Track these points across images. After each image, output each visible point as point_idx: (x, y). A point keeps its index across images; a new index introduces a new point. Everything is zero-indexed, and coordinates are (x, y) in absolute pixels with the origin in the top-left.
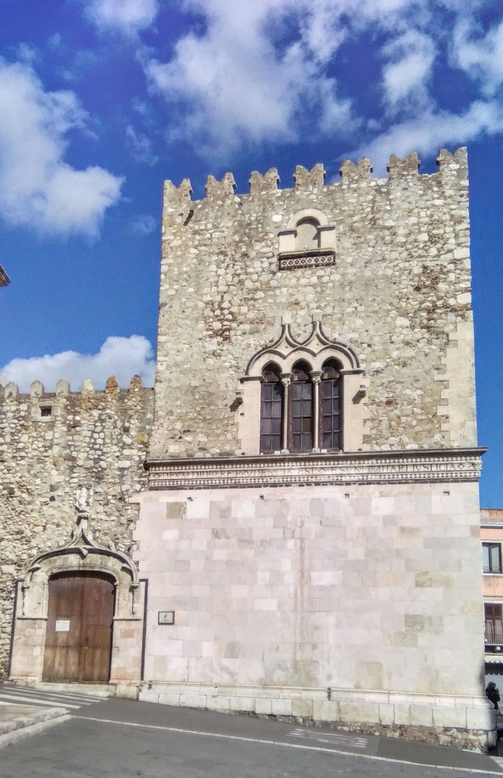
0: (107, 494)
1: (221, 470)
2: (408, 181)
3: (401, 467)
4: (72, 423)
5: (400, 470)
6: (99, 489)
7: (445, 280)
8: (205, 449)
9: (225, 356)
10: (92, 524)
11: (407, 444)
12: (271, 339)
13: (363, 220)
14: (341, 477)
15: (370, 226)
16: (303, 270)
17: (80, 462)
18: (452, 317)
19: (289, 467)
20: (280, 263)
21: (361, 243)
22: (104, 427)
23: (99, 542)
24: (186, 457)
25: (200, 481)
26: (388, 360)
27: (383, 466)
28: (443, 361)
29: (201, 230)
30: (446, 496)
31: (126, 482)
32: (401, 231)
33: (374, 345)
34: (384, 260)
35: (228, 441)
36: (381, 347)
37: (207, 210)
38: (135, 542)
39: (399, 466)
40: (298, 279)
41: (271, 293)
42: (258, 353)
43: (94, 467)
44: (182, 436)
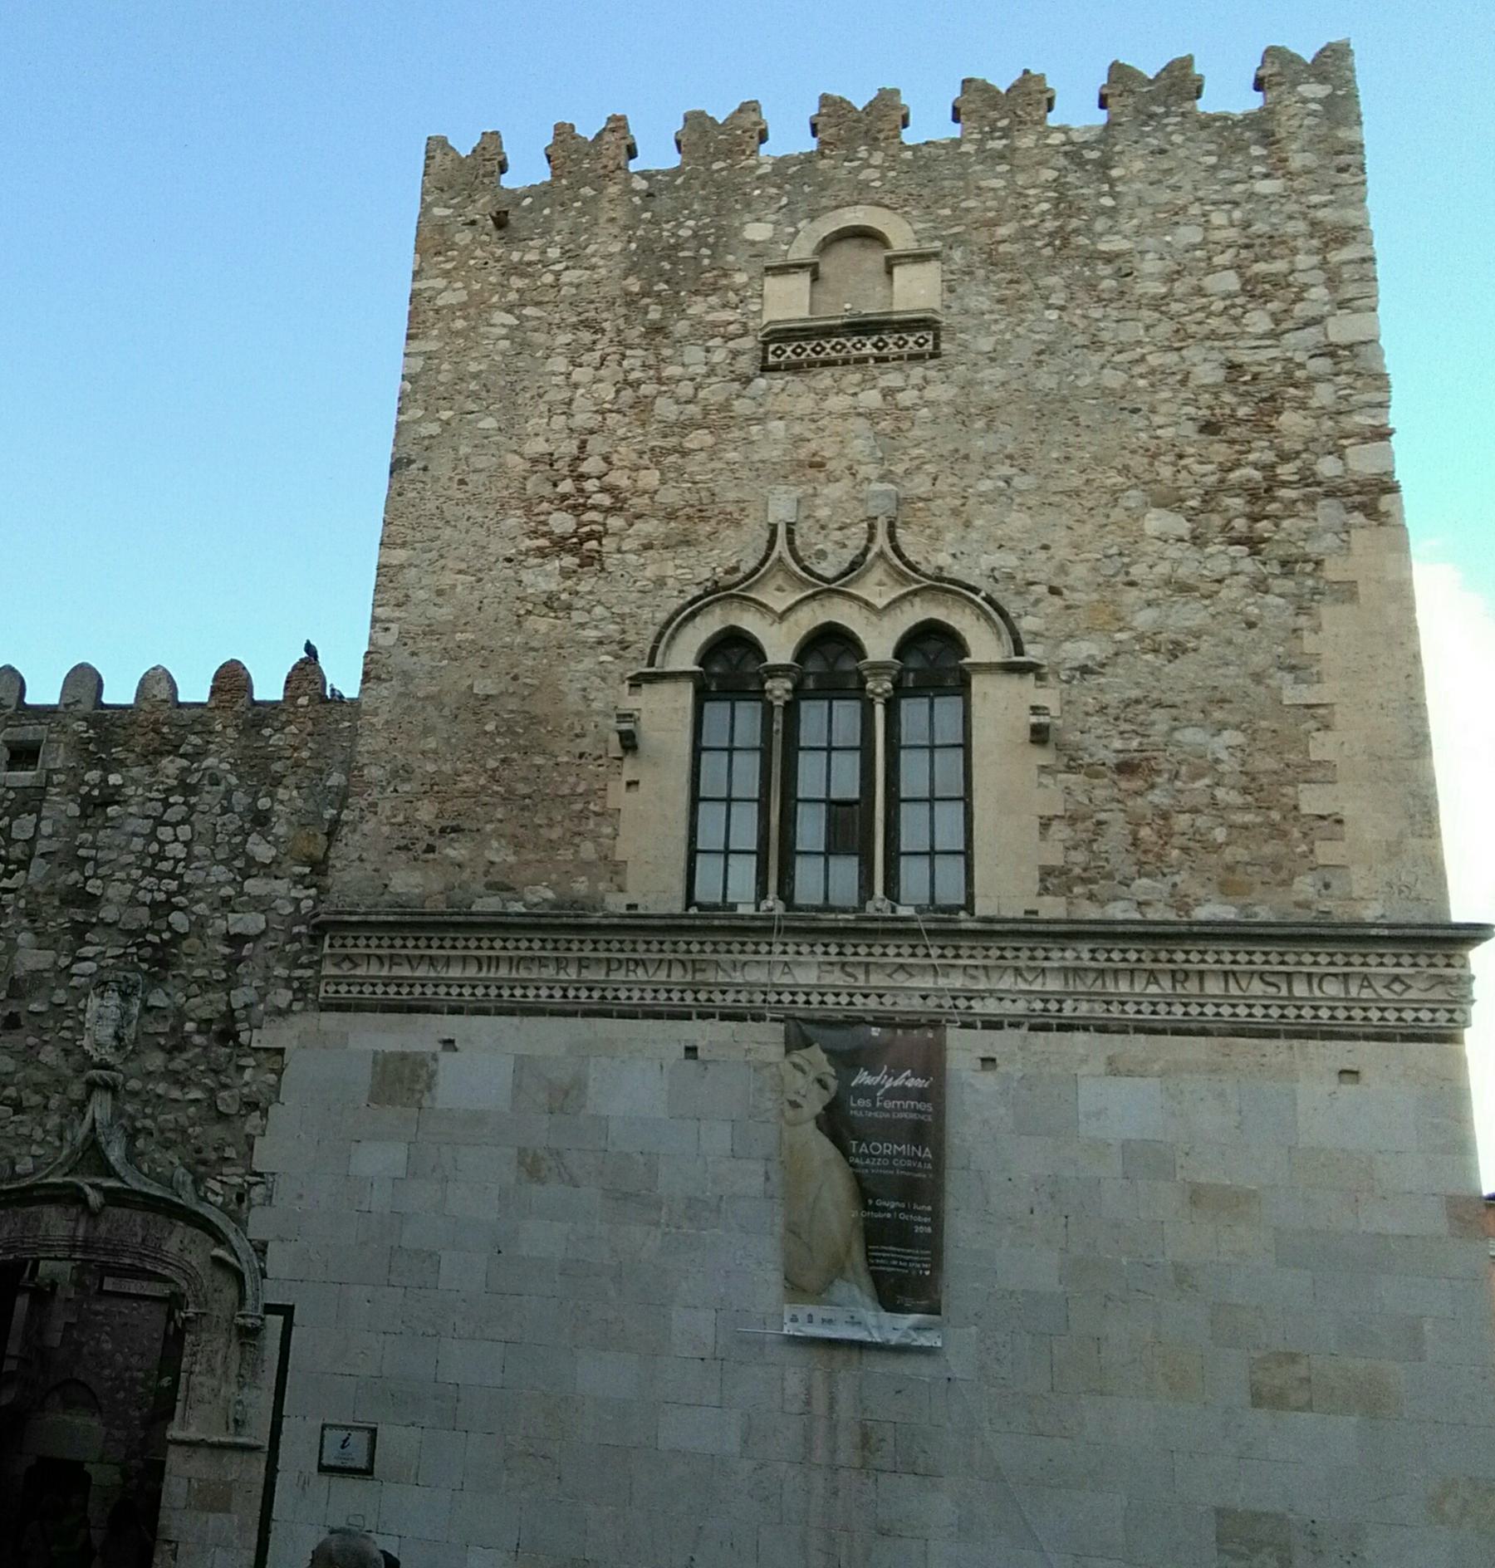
0: (181, 1015)
1: (555, 954)
2: (1169, 129)
3: (1180, 976)
4: (96, 793)
5: (1179, 990)
6: (157, 999)
7: (1302, 405)
8: (509, 889)
9: (582, 609)
10: (129, 1108)
11: (1198, 902)
12: (733, 563)
13: (1024, 235)
14: (969, 999)
15: (1048, 251)
16: (838, 371)
17: (109, 913)
18: (1328, 511)
19: (785, 958)
20: (765, 350)
21: (1023, 297)
22: (192, 808)
23: (145, 1168)
24: (443, 907)
25: (487, 987)
26: (1119, 636)
27: (1116, 971)
28: (1309, 643)
29: (529, 264)
30: (1348, 1088)
31: (246, 981)
32: (1150, 265)
33: (1072, 589)
34: (1096, 345)
35: (585, 866)
36: (1095, 596)
37: (547, 211)
38: (261, 1175)
39: (1173, 972)
40: (824, 395)
41: (736, 434)
42: (691, 603)
43: (149, 929)
44: (437, 843)
